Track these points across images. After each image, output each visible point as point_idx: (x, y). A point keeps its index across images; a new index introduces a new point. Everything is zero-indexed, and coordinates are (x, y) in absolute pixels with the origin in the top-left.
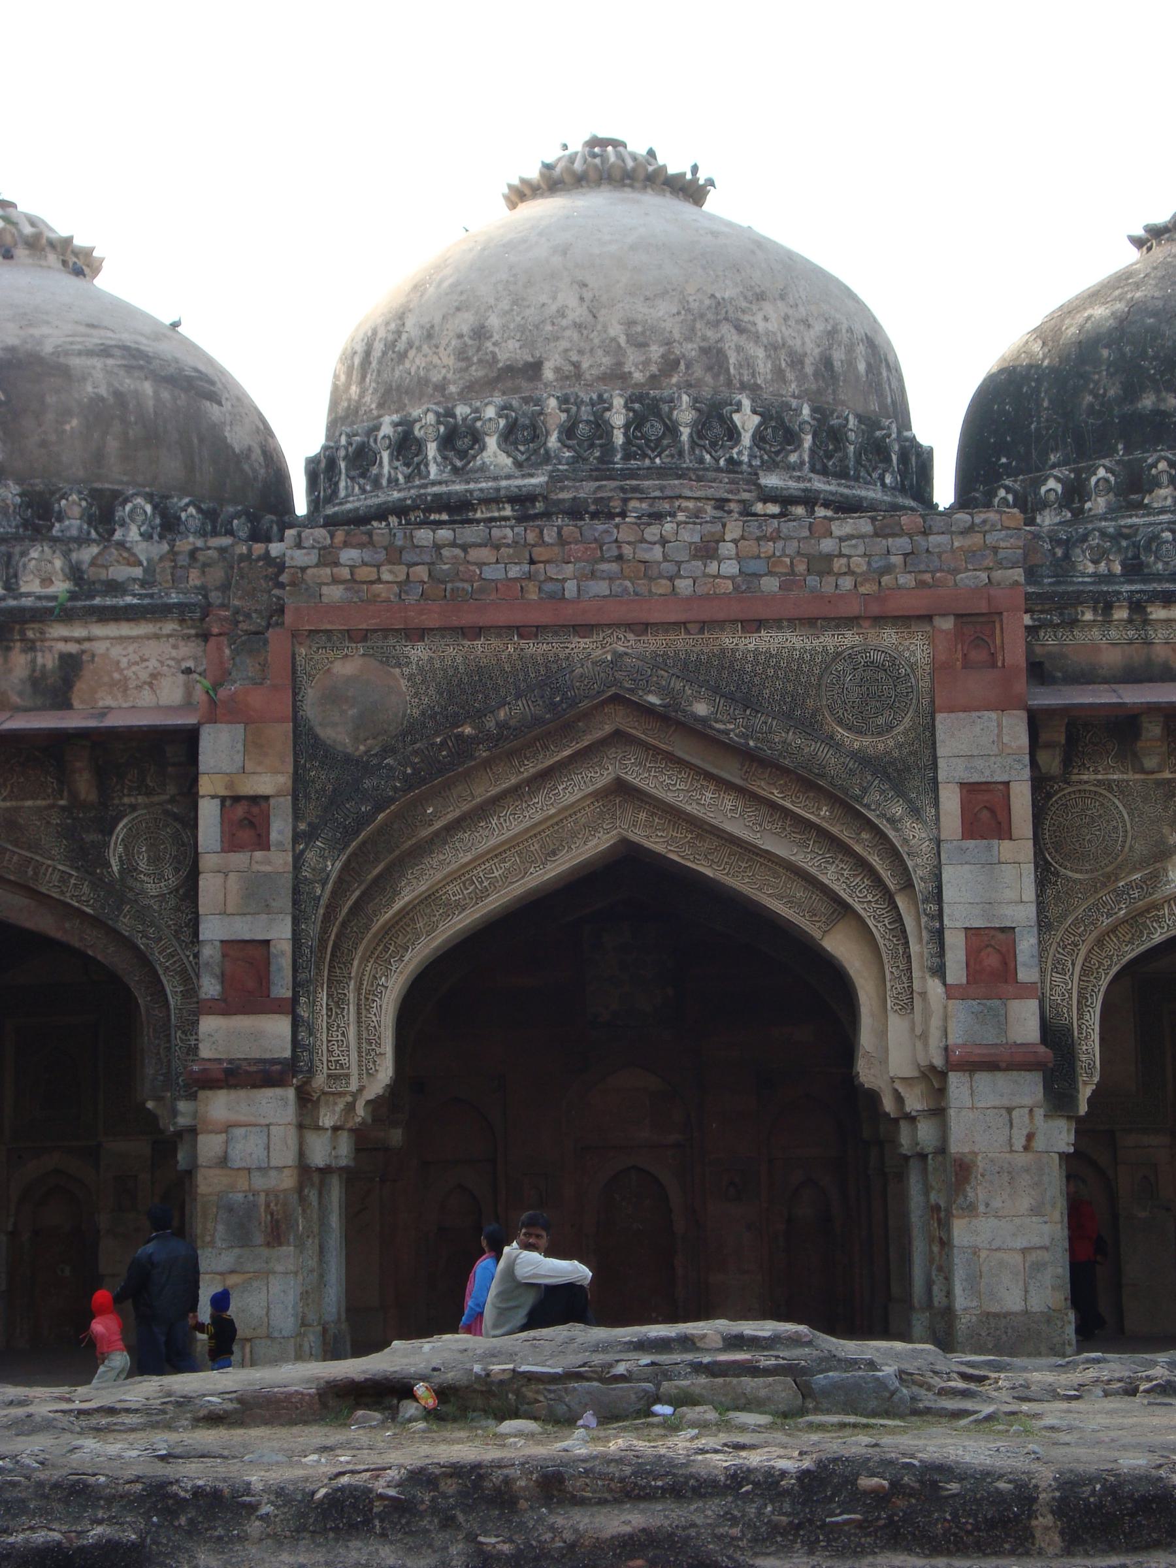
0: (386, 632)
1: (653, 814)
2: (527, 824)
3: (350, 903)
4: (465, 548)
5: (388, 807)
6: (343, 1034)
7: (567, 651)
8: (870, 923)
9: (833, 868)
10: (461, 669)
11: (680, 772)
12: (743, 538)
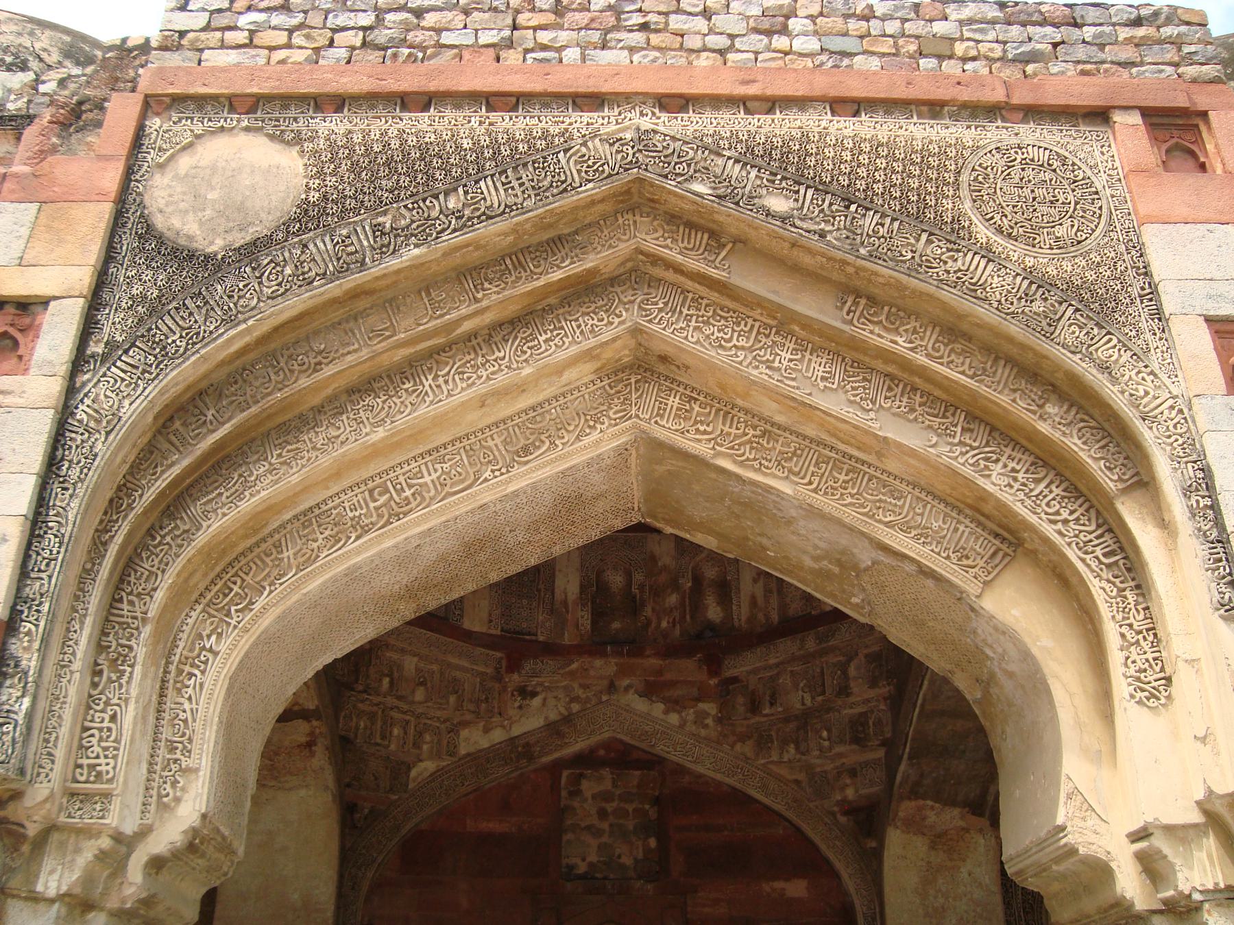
0: (286, 100)
1: (692, 399)
2: (480, 388)
3: (161, 484)
4: (419, 13)
5: (245, 321)
6: (113, 718)
7: (563, 126)
8: (1072, 554)
9: (998, 468)
10: (395, 144)
11: (739, 324)
12: (821, 14)
